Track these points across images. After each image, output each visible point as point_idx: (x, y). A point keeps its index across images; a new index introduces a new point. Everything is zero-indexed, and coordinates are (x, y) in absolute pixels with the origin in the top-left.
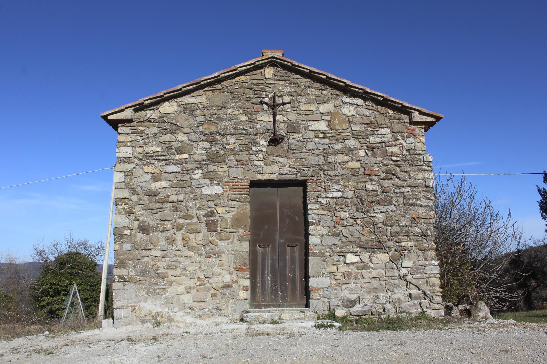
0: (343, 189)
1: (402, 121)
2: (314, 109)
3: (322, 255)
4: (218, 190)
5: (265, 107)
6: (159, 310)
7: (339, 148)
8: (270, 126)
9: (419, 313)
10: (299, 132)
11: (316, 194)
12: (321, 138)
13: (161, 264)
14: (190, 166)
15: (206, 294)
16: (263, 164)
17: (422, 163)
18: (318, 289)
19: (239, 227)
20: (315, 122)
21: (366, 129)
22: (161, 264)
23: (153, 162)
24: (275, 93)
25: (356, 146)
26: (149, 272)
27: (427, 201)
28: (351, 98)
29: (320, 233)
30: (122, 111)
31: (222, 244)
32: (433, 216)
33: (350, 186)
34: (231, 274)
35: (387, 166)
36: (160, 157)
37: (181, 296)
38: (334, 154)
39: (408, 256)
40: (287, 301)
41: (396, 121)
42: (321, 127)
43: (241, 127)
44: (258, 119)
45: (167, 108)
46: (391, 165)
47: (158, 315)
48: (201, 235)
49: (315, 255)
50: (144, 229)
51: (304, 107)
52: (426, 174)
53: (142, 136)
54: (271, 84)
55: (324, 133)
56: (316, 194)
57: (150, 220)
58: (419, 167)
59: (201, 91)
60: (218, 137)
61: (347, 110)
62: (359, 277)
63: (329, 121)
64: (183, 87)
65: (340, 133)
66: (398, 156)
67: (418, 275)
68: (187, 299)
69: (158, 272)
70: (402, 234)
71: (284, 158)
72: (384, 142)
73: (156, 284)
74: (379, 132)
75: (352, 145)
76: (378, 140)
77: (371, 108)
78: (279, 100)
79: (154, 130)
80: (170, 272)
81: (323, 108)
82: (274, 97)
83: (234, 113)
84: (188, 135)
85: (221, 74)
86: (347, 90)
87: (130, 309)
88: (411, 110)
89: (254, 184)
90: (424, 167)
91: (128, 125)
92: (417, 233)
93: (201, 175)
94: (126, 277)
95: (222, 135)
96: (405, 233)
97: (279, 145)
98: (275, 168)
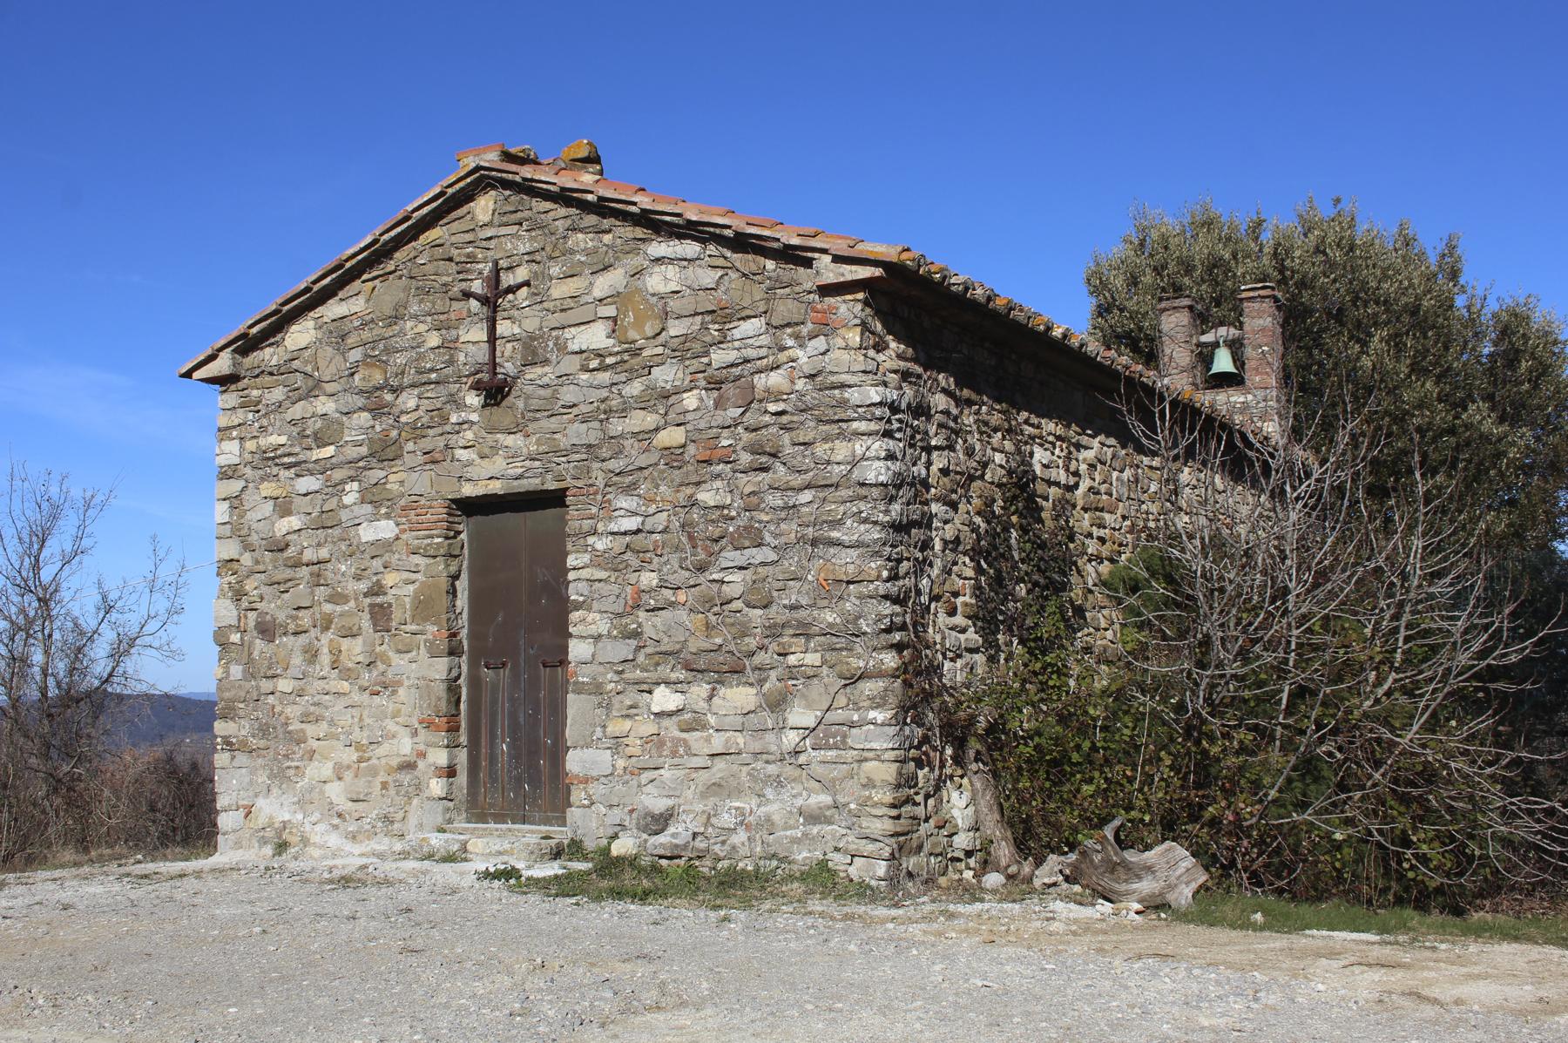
0: (643, 508)
1: (797, 289)
2: (581, 291)
3: (597, 689)
4: (385, 529)
5: (474, 304)
6: (287, 817)
7: (635, 393)
8: (482, 354)
9: (815, 862)
10: (546, 362)
11: (587, 524)
12: (594, 370)
13: (293, 711)
14: (338, 475)
15: (370, 782)
16: (475, 456)
17: (851, 414)
18: (586, 780)
19: (426, 619)
20: (583, 327)
21: (704, 327)
22: (293, 711)
23: (275, 470)
24: (496, 263)
25: (676, 383)
26: (274, 728)
27: (862, 527)
28: (672, 243)
29: (593, 630)
30: (212, 358)
31: (398, 661)
32: (874, 574)
33: (658, 498)
34: (415, 733)
35: (755, 430)
36: (286, 460)
37: (328, 786)
38: (624, 412)
39: (803, 696)
40: (539, 807)
41: (782, 291)
42: (595, 339)
43: (428, 366)
44: (461, 340)
45: (300, 334)
46: (766, 426)
47: (285, 828)
48: (359, 640)
49: (580, 689)
50: (267, 630)
51: (560, 290)
52: (857, 446)
53: (258, 411)
54: (490, 238)
55: (601, 356)
56: (587, 524)
57: (276, 608)
58: (844, 425)
59: (357, 284)
60: (389, 397)
61: (657, 281)
62: (681, 750)
63: (615, 320)
64: (314, 282)
65: (636, 353)
66: (785, 397)
67: (830, 753)
68: (335, 792)
69: (290, 728)
70: (791, 632)
71: (518, 435)
72: (747, 361)
73: (286, 756)
74: (737, 334)
75: (667, 382)
76: (732, 356)
77: (721, 262)
78: (508, 280)
79: (278, 394)
80: (310, 730)
81: (603, 284)
82: (497, 271)
83: (416, 331)
84: (335, 398)
85: (381, 235)
86: (651, 223)
87: (242, 812)
88: (809, 255)
89: (468, 507)
90: (855, 425)
91: (233, 387)
92: (830, 625)
93: (357, 495)
94: (234, 740)
95: (395, 391)
96: (798, 628)
97: (504, 404)
98: (498, 464)
